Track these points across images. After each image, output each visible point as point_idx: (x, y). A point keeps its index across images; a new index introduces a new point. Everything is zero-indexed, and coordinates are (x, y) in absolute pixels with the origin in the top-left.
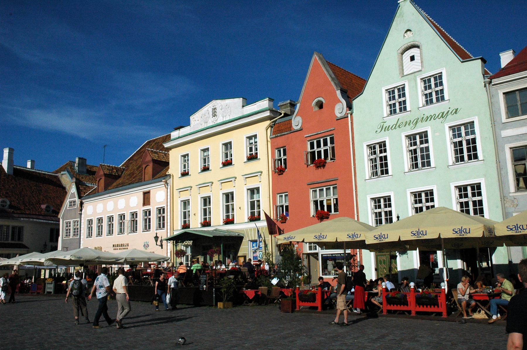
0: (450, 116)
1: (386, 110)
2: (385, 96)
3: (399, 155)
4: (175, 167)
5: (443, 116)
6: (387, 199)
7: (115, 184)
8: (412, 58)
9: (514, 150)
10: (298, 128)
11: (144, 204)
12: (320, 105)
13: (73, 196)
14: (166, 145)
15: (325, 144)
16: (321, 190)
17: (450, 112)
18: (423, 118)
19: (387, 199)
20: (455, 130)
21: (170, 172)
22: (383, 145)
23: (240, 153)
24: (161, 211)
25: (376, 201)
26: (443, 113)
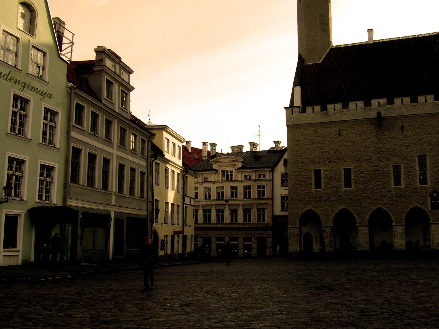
0: (46, 97)
17: (47, 94)
18: (29, 85)
26: (43, 92)
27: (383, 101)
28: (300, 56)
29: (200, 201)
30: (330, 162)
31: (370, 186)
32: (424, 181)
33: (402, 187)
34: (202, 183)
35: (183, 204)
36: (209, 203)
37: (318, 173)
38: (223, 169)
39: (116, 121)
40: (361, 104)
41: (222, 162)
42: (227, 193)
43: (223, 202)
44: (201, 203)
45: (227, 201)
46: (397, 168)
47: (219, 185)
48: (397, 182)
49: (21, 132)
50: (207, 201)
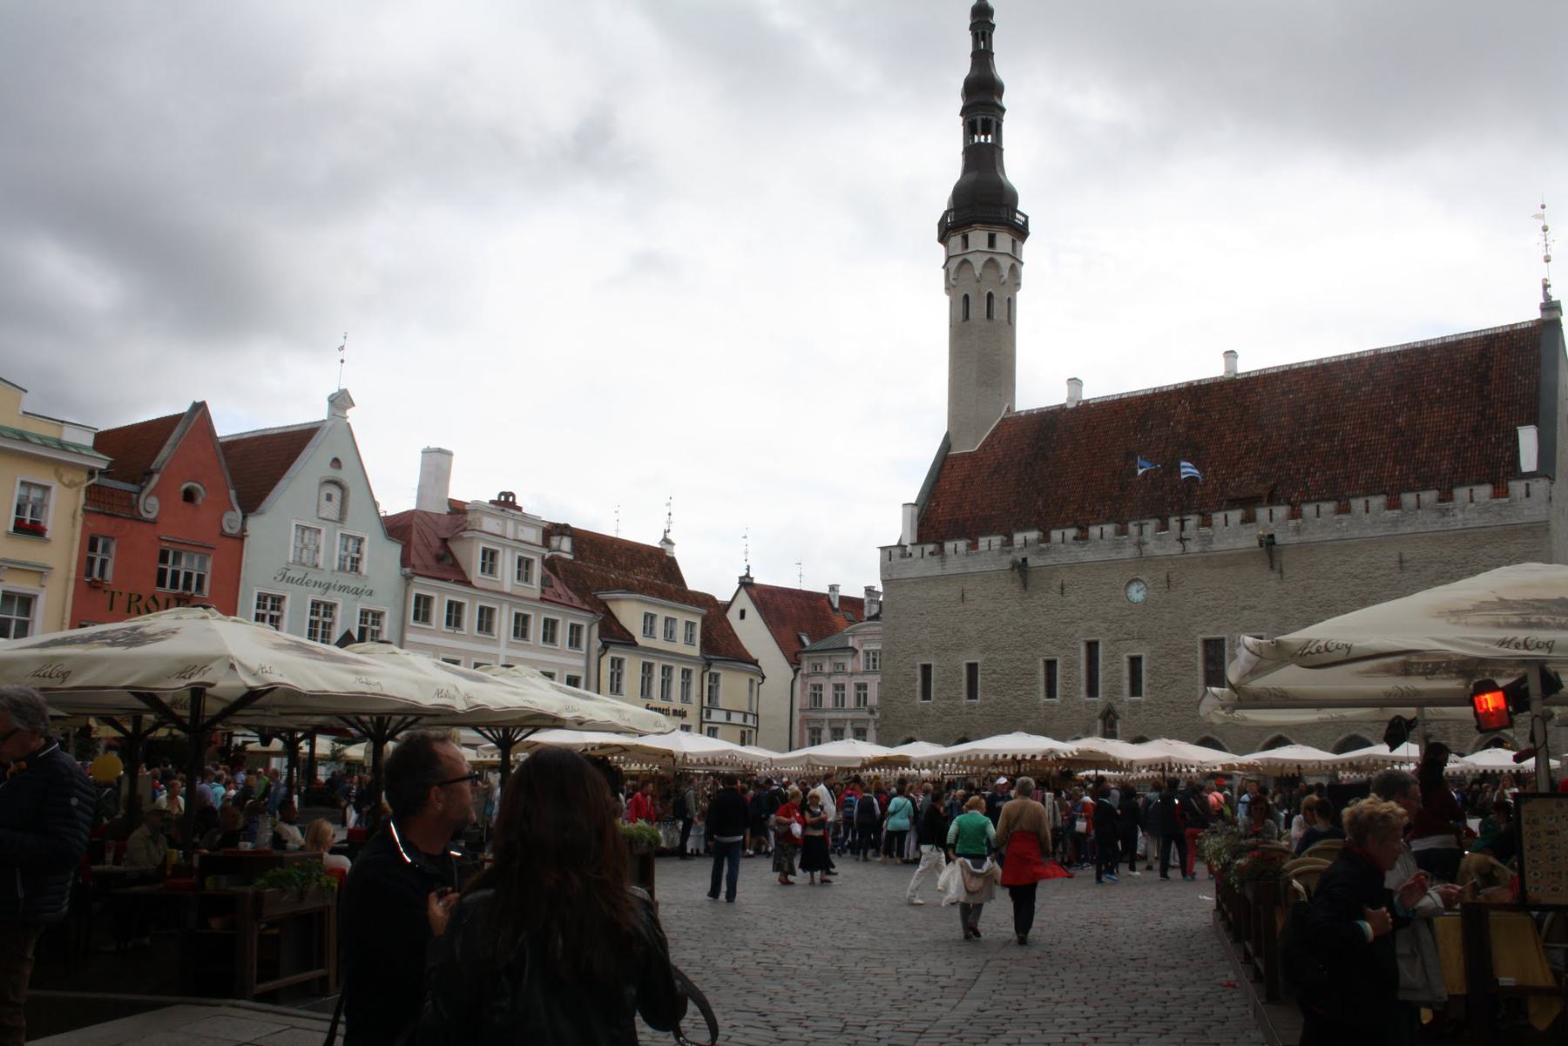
5: (357, 592)
8: (329, 497)
10: (152, 516)
12: (189, 496)
27: (1033, 535)
28: (947, 436)
29: (827, 710)
30: (946, 650)
31: (1007, 698)
32: (1092, 690)
33: (1056, 700)
34: (830, 675)
35: (702, 722)
36: (841, 715)
37: (926, 669)
38: (866, 647)
39: (506, 607)
40: (996, 541)
41: (865, 634)
42: (873, 696)
43: (866, 715)
44: (827, 715)
45: (872, 712)
46: (1050, 665)
47: (861, 680)
48: (1051, 693)
50: (838, 710)
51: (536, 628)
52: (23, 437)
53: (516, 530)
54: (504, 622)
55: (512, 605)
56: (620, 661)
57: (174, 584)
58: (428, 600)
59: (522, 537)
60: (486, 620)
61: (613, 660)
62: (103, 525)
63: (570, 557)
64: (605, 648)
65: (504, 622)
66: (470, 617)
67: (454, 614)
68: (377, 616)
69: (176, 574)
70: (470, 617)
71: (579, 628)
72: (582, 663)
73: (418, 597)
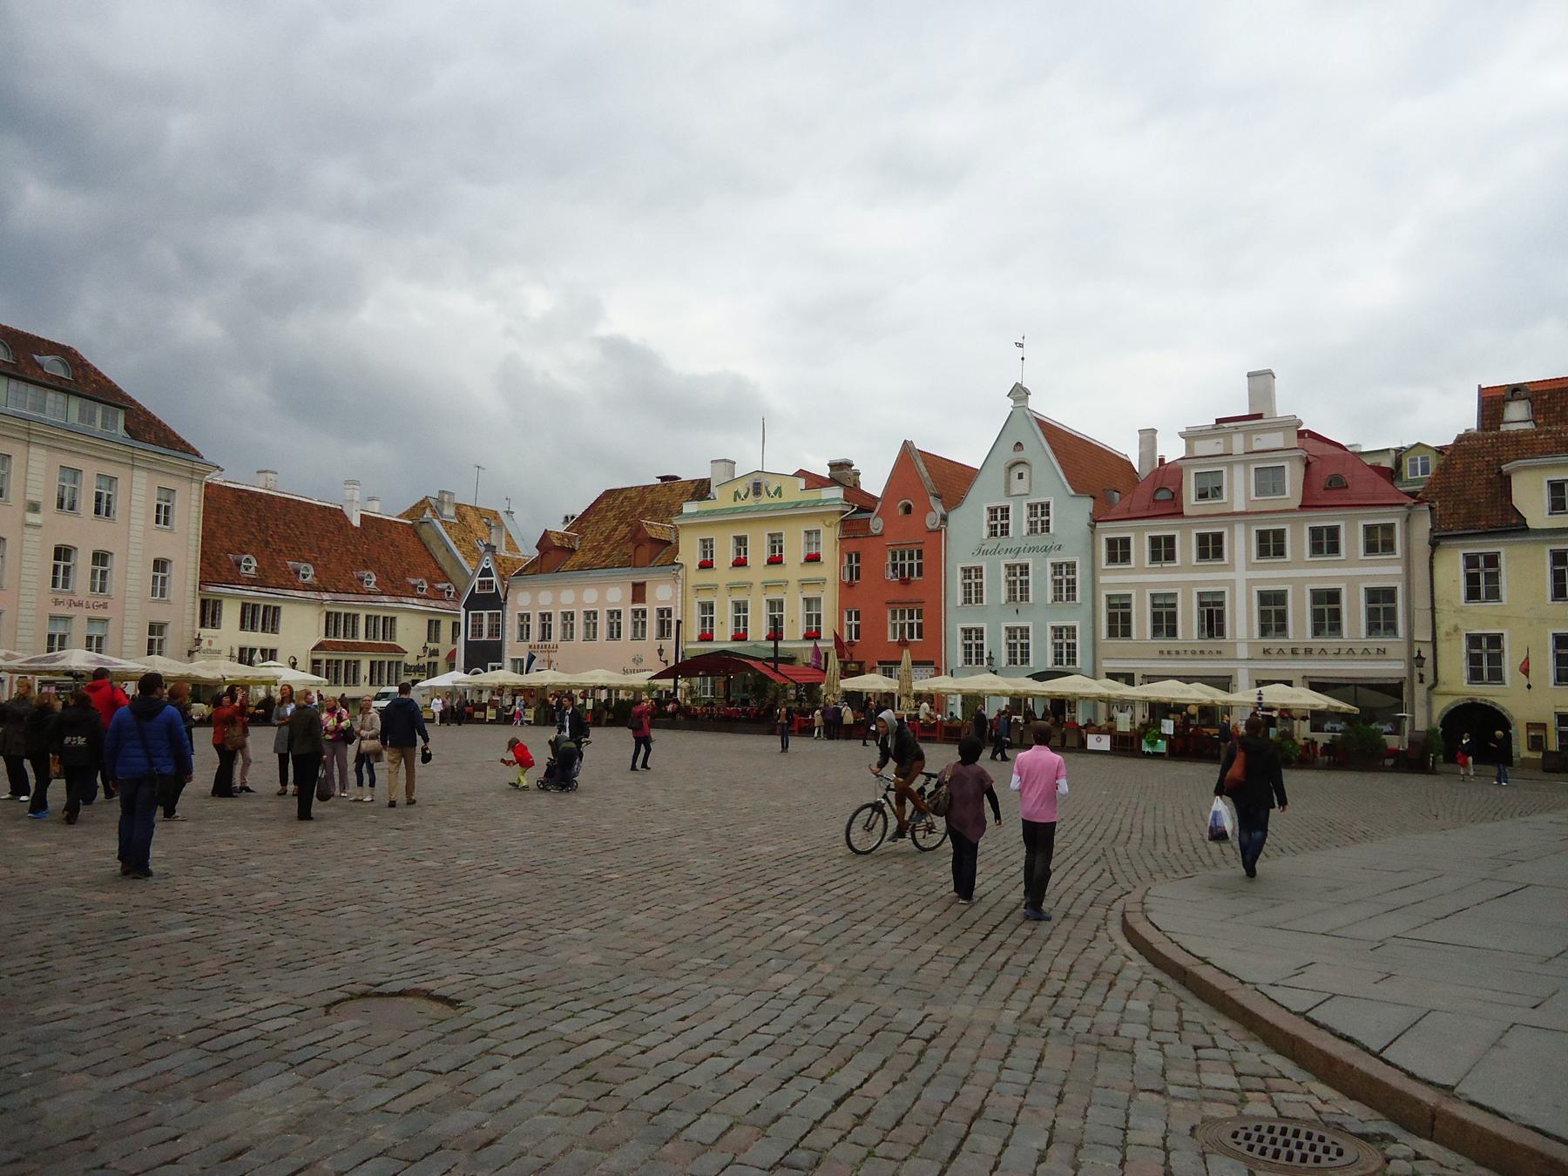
1: (986, 531)
2: (986, 515)
3: (996, 587)
4: (689, 553)
6: (980, 632)
7: (570, 563)
8: (1021, 476)
9: (1109, 597)
11: (634, 601)
12: (908, 509)
13: (486, 572)
14: (677, 521)
15: (911, 557)
16: (902, 613)
19: (980, 632)
20: (1057, 567)
21: (680, 559)
22: (979, 570)
23: (794, 550)
24: (664, 613)
25: (967, 632)
39: (1240, 530)
49: (1025, 598)
51: (1298, 540)
52: (797, 505)
53: (1248, 441)
54: (1240, 543)
55: (1248, 524)
56: (1492, 560)
57: (903, 573)
58: (1126, 542)
59: (1255, 448)
60: (1211, 547)
61: (1471, 561)
62: (853, 545)
63: (1529, 426)
64: (1434, 544)
65: (1240, 543)
66: (1187, 547)
67: (1163, 550)
68: (1071, 567)
69: (903, 566)
70: (1187, 547)
71: (1389, 529)
72: (1398, 570)
73: (1111, 543)
